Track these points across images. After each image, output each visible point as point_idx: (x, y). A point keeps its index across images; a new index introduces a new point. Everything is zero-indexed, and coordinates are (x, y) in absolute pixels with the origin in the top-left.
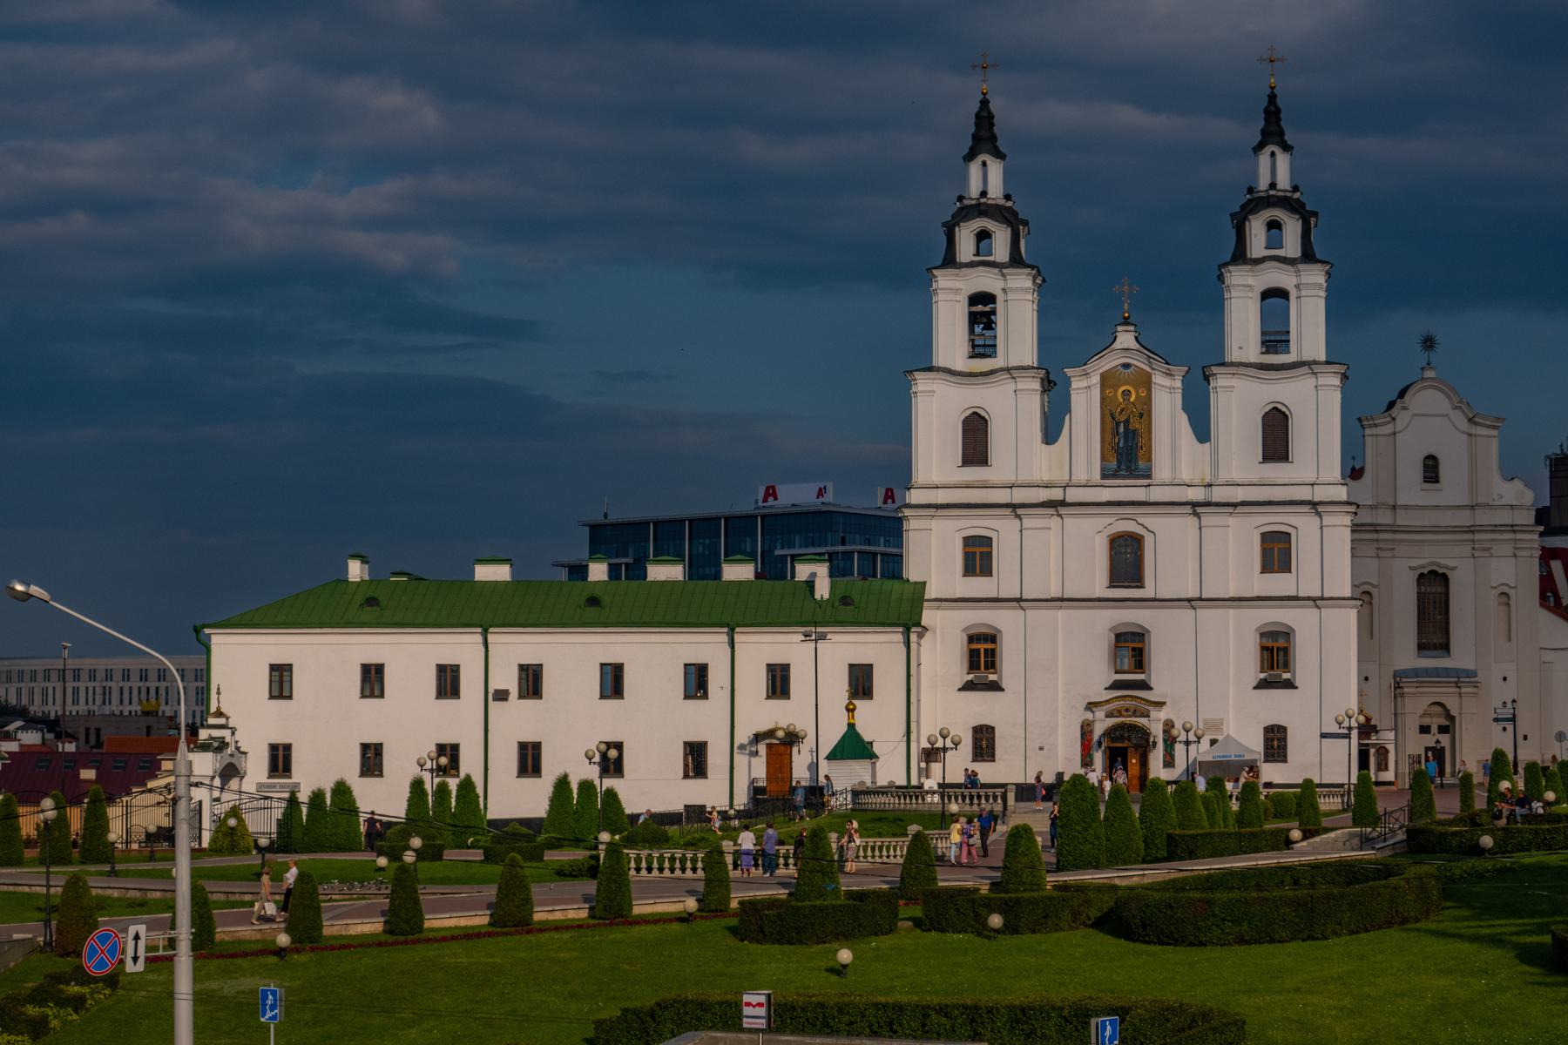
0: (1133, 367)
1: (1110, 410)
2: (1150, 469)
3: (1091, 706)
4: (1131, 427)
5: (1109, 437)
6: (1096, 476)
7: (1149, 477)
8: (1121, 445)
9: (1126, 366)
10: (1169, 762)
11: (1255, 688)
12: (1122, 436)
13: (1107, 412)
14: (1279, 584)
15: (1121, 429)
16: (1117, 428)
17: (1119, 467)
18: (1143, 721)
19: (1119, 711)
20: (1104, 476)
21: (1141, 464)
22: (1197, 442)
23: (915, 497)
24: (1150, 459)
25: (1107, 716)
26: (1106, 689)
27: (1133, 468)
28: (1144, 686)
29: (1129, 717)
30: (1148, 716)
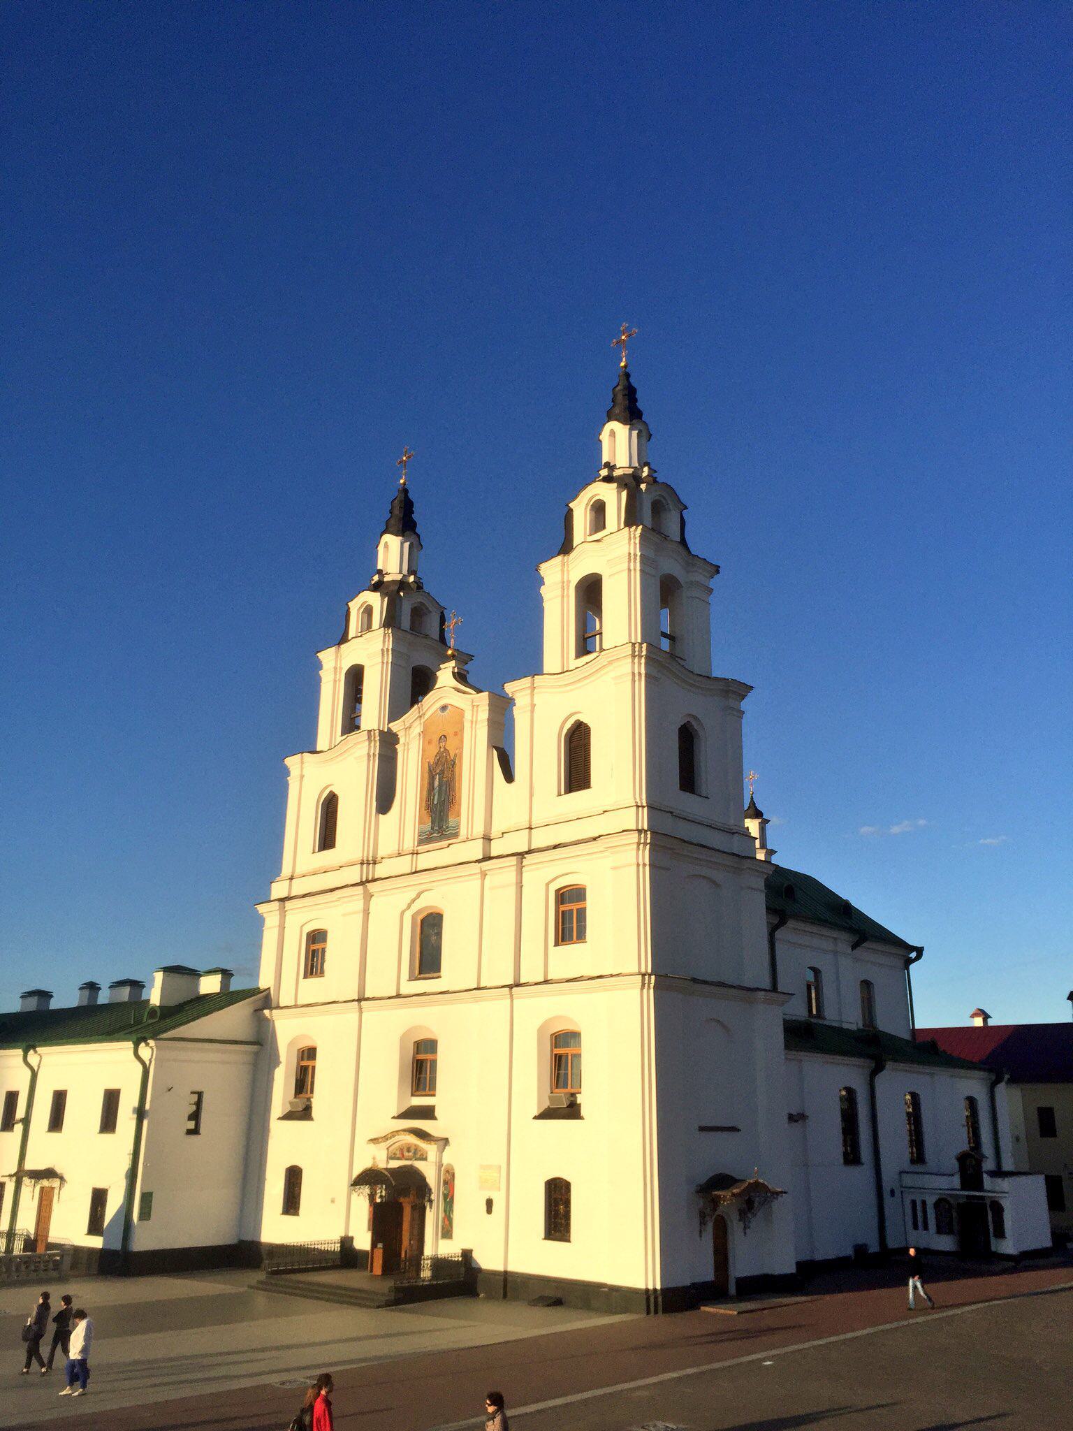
0: (449, 707)
1: (429, 763)
2: (458, 827)
3: (374, 1141)
4: (447, 774)
5: (425, 793)
6: (410, 842)
7: (456, 835)
8: (435, 803)
9: (444, 708)
10: (447, 1233)
11: (536, 1118)
12: (436, 790)
13: (426, 766)
14: (570, 959)
15: (436, 783)
16: (433, 783)
17: (432, 828)
18: (419, 1165)
19: (402, 1150)
20: (421, 842)
21: (452, 821)
22: (504, 780)
23: (278, 890)
24: (459, 815)
25: (392, 1157)
26: (394, 1118)
27: (444, 827)
28: (427, 1113)
29: (411, 1160)
30: (425, 1159)
